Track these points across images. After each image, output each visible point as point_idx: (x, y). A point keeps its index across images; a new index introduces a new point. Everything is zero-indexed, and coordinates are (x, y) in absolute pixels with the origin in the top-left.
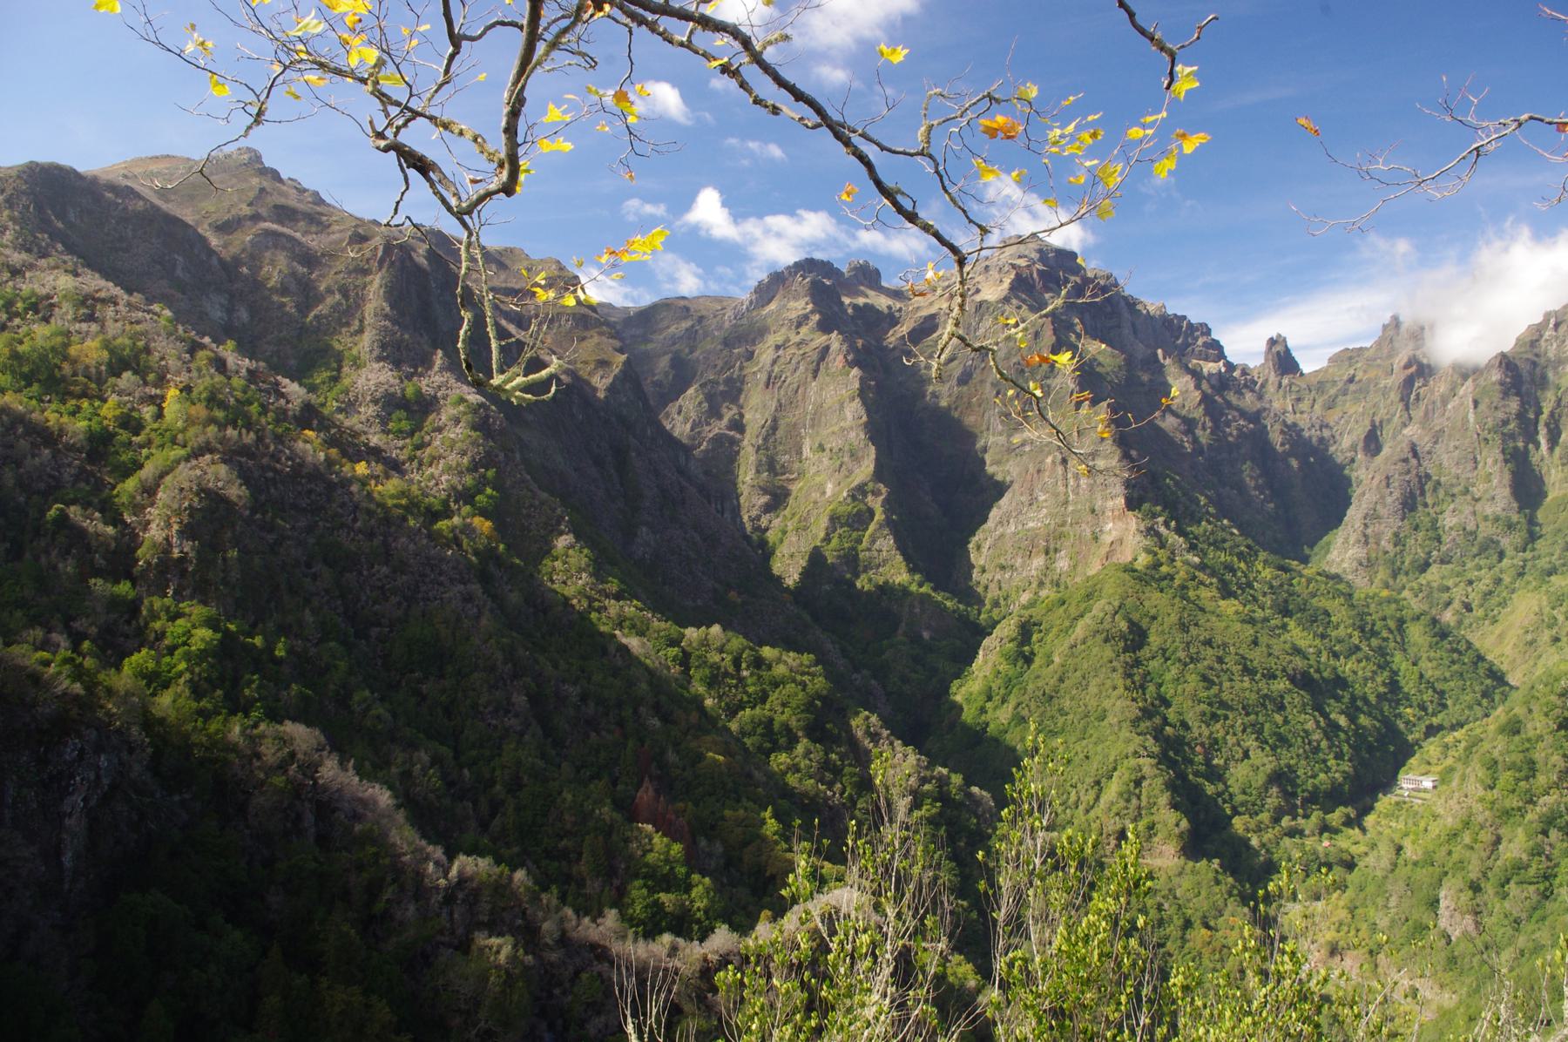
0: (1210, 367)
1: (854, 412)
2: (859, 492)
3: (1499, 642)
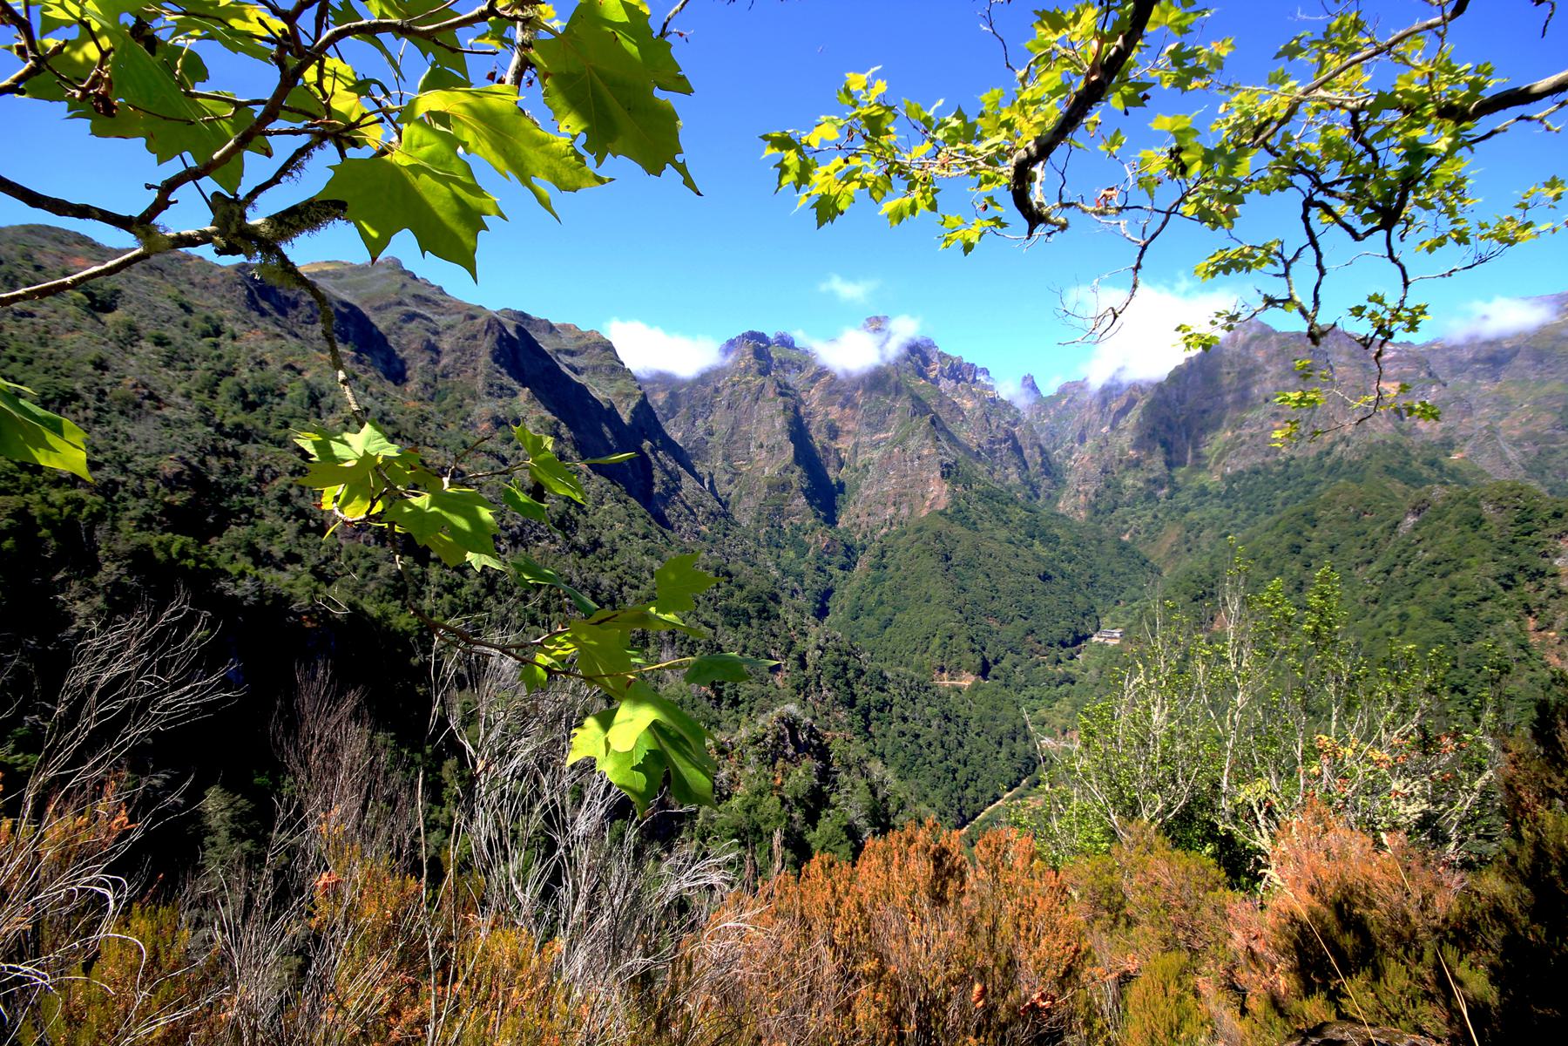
1: (779, 422)
2: (786, 469)
3: (1156, 553)
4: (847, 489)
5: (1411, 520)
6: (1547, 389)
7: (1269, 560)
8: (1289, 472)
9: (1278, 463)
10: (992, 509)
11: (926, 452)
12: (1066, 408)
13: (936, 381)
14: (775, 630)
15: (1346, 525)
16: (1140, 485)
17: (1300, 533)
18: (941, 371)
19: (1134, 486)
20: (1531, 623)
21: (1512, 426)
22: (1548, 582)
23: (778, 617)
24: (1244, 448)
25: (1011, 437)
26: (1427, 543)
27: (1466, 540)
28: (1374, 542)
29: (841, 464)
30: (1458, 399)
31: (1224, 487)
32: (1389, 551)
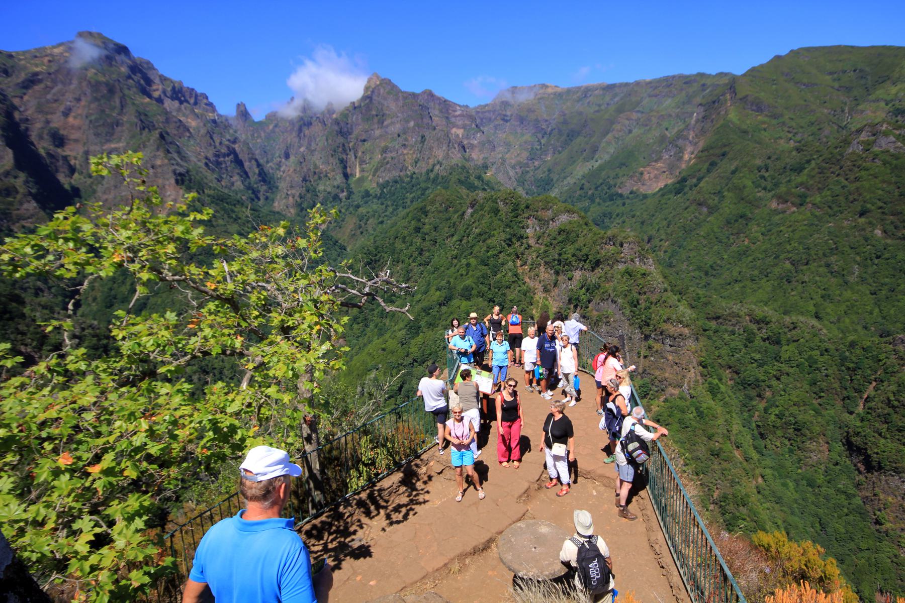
0: (211, 116)
4: (83, 194)
5: (470, 211)
6: (524, 138)
7: (405, 238)
8: (413, 182)
9: (407, 176)
10: (224, 209)
11: (158, 162)
12: (273, 131)
13: (160, 101)
14: (22, 327)
15: (441, 215)
16: (329, 189)
17: (419, 220)
18: (164, 92)
19: (325, 191)
20: (519, 263)
21: (511, 158)
22: (524, 241)
23: (23, 316)
24: (388, 166)
25: (233, 152)
26: (477, 224)
27: (492, 222)
28: (454, 224)
29: (72, 170)
30: (489, 142)
31: (379, 192)
32: (461, 228)
